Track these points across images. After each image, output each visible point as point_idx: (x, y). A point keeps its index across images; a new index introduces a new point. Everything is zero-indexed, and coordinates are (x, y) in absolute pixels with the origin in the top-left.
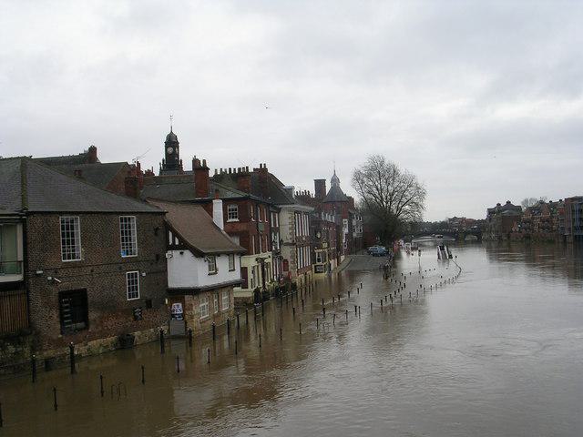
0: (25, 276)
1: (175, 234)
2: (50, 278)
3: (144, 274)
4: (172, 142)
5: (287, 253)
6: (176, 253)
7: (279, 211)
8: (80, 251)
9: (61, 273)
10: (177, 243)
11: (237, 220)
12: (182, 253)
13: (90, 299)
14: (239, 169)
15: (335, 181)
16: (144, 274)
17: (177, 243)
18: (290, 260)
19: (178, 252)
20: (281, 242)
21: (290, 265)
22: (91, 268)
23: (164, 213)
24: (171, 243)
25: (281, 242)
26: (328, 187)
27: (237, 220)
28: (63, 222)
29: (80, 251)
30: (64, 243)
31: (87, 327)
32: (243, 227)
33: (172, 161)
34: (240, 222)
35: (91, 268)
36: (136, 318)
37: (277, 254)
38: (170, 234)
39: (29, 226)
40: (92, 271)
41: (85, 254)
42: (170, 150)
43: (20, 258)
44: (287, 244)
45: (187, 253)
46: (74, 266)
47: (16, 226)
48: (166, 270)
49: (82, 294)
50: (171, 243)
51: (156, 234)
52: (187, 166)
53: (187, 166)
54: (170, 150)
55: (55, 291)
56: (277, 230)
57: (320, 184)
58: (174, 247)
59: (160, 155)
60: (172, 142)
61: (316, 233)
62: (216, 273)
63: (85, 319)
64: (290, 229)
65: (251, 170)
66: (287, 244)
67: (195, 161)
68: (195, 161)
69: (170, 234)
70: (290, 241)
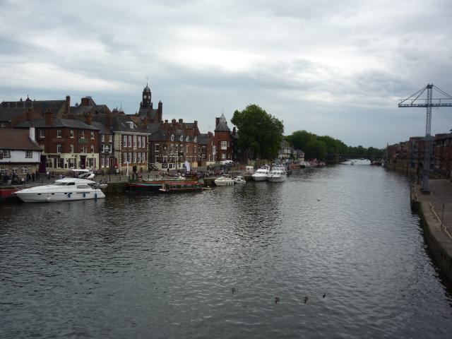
4: (147, 93)
5: (117, 155)
7: (114, 134)
20: (113, 149)
25: (113, 149)
32: (64, 140)
33: (146, 104)
42: (145, 97)
52: (155, 107)
53: (155, 107)
56: (113, 143)
60: (147, 93)
67: (160, 104)
68: (160, 104)
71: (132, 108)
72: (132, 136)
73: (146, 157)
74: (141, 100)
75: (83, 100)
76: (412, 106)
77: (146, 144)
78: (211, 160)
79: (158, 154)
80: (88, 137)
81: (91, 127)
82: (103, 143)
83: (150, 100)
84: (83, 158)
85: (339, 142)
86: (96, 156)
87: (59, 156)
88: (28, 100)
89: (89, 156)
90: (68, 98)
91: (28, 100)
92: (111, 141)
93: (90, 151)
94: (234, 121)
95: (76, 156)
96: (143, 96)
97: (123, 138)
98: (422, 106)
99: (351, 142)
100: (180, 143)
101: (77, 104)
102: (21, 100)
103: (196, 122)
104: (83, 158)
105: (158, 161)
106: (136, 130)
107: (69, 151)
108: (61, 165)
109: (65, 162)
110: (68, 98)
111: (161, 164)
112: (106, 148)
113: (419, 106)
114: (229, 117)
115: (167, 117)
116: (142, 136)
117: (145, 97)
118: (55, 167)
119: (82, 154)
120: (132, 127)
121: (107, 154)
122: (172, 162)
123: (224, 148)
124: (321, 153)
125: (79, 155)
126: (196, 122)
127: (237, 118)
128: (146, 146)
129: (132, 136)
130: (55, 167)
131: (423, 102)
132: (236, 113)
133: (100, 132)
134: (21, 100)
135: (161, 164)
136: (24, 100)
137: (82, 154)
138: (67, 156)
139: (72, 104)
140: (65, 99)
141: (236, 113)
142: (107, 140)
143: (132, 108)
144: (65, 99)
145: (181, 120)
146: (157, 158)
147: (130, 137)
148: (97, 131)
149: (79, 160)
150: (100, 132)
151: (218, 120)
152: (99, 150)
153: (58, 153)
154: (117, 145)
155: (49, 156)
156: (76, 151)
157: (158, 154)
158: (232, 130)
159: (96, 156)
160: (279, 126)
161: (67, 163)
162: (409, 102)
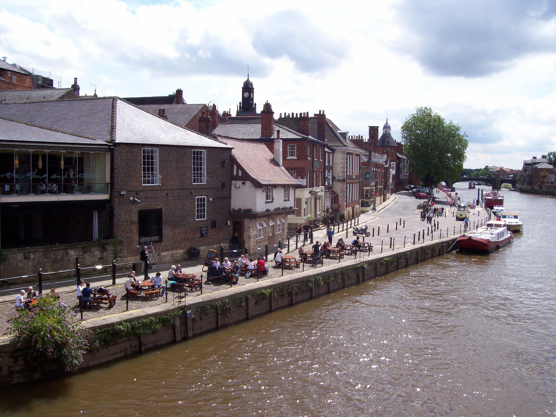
0: (111, 195)
1: (240, 167)
2: (132, 198)
3: (211, 199)
4: (248, 88)
5: (338, 188)
6: (239, 183)
8: (158, 177)
9: (142, 194)
10: (240, 174)
11: (295, 158)
12: (243, 183)
13: (164, 217)
14: (301, 114)
15: (387, 127)
16: (211, 199)
17: (240, 174)
18: (340, 195)
19: (241, 182)
21: (340, 199)
22: (166, 192)
23: (230, 149)
24: (235, 173)
25: (333, 178)
26: (380, 134)
28: (144, 152)
29: (158, 177)
30: (144, 170)
31: (161, 240)
32: (300, 164)
33: (247, 104)
34: (298, 159)
35: (166, 192)
36: (202, 235)
37: (329, 189)
38: (235, 167)
39: (116, 154)
40: (167, 194)
41: (162, 180)
42: (247, 95)
43: (108, 180)
44: (339, 180)
45: (248, 183)
46: (153, 189)
47: (105, 154)
48: (230, 197)
49: (158, 213)
50: (235, 173)
51: (223, 166)
52: (259, 109)
53: (259, 109)
54: (247, 95)
55: (135, 209)
56: (332, 168)
57: (373, 130)
58: (237, 178)
59: (238, 98)
60: (248, 88)
62: (272, 202)
63: (159, 233)
64: (342, 167)
65: (311, 115)
66: (339, 180)
67: (267, 107)
68: (267, 107)
69: (235, 167)
70: (342, 178)
72: (351, 154)
74: (240, 100)
83: (253, 100)
96: (243, 92)
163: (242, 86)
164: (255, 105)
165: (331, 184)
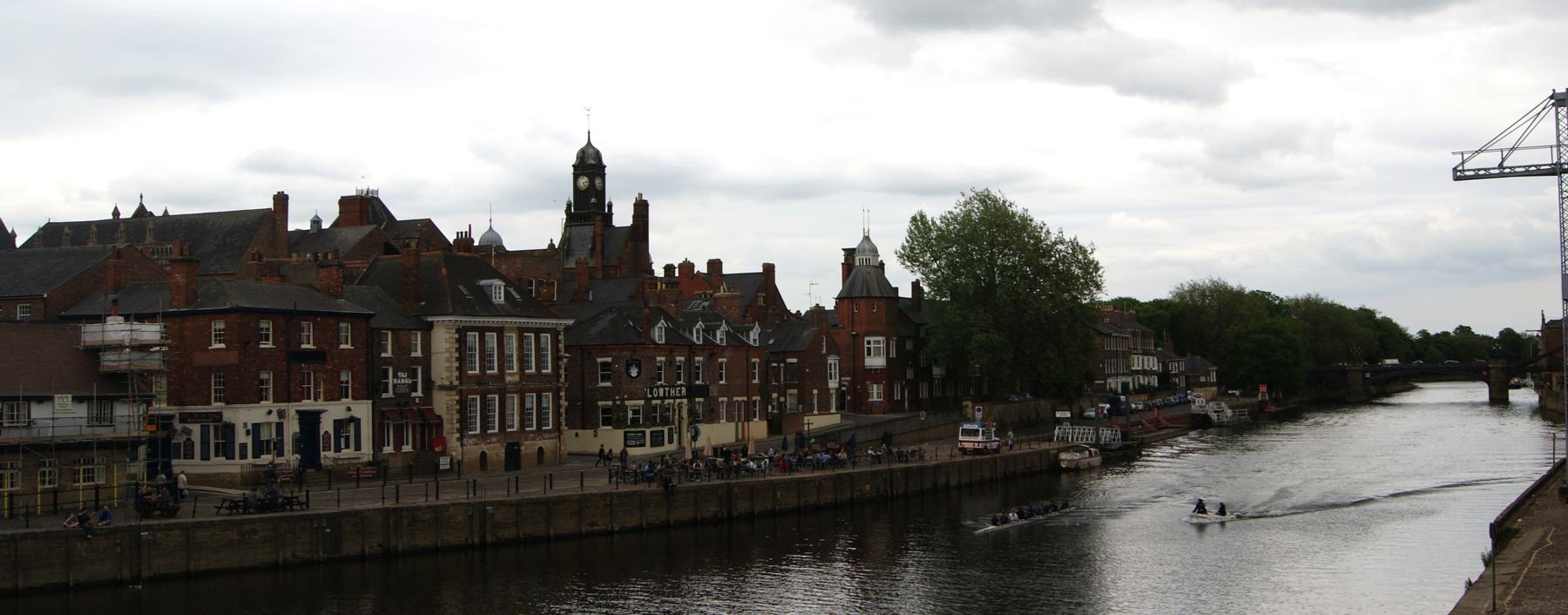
4: (589, 165)
5: (443, 404)
7: (431, 326)
11: (223, 346)
18: (445, 417)
20: (429, 385)
21: (446, 426)
27: (223, 346)
42: (583, 182)
44: (442, 388)
52: (623, 217)
53: (623, 217)
56: (426, 361)
60: (589, 165)
61: (628, 367)
67: (641, 208)
68: (641, 208)
71: (536, 228)
72: (500, 331)
73: (557, 407)
74: (568, 194)
75: (344, 202)
76: (1503, 172)
77: (557, 359)
78: (824, 409)
79: (606, 393)
80: (328, 338)
81: (344, 305)
82: (388, 361)
83: (601, 194)
84: (310, 421)
85: (1366, 316)
86: (363, 410)
87: (218, 416)
88: (141, 211)
89: (333, 412)
90: (281, 200)
91: (141, 211)
92: (419, 354)
93: (336, 393)
94: (909, 256)
95: (281, 414)
96: (576, 177)
97: (461, 341)
98: (1539, 172)
99: (1420, 314)
100: (692, 349)
101: (316, 222)
102: (116, 213)
103: (769, 269)
104: (310, 421)
105: (606, 422)
106: (512, 308)
107: (258, 397)
108: (226, 449)
109: (242, 437)
110: (281, 200)
111: (620, 433)
112: (395, 381)
113: (1528, 172)
114: (890, 246)
115: (664, 252)
116: (538, 332)
117: (583, 182)
118: (205, 457)
119: (308, 405)
120: (499, 298)
121: (403, 399)
122: (665, 421)
123: (876, 361)
124: (1286, 361)
125: (292, 409)
126: (769, 269)
127: (924, 239)
128: (556, 367)
129: (500, 331)
130: (205, 457)
131: (1545, 158)
132: (920, 224)
133: (374, 323)
134: (116, 213)
135: (620, 433)
136: (127, 212)
137: (308, 405)
138: (243, 416)
139: (298, 222)
140: (269, 204)
141: (920, 224)
142: (402, 348)
143: (536, 228)
144: (269, 204)
145: (715, 265)
146: (606, 410)
147: (492, 338)
148: (368, 317)
149: (292, 427)
150: (374, 323)
151: (850, 253)
152: (370, 388)
153: (216, 406)
154: (443, 367)
155: (184, 418)
156: (286, 394)
157: (606, 393)
158: (905, 292)
159: (363, 410)
160: (1077, 269)
161: (249, 441)
162: (1490, 160)
163: (573, 160)
164: (610, 206)
165: (419, 393)
